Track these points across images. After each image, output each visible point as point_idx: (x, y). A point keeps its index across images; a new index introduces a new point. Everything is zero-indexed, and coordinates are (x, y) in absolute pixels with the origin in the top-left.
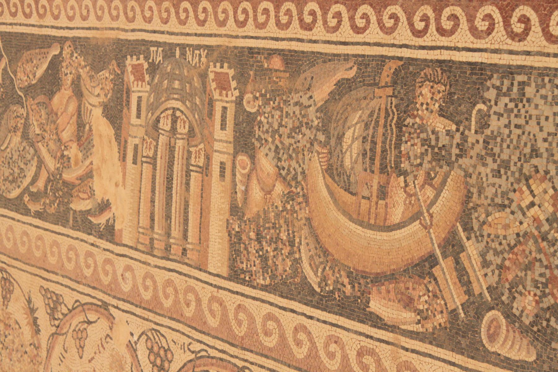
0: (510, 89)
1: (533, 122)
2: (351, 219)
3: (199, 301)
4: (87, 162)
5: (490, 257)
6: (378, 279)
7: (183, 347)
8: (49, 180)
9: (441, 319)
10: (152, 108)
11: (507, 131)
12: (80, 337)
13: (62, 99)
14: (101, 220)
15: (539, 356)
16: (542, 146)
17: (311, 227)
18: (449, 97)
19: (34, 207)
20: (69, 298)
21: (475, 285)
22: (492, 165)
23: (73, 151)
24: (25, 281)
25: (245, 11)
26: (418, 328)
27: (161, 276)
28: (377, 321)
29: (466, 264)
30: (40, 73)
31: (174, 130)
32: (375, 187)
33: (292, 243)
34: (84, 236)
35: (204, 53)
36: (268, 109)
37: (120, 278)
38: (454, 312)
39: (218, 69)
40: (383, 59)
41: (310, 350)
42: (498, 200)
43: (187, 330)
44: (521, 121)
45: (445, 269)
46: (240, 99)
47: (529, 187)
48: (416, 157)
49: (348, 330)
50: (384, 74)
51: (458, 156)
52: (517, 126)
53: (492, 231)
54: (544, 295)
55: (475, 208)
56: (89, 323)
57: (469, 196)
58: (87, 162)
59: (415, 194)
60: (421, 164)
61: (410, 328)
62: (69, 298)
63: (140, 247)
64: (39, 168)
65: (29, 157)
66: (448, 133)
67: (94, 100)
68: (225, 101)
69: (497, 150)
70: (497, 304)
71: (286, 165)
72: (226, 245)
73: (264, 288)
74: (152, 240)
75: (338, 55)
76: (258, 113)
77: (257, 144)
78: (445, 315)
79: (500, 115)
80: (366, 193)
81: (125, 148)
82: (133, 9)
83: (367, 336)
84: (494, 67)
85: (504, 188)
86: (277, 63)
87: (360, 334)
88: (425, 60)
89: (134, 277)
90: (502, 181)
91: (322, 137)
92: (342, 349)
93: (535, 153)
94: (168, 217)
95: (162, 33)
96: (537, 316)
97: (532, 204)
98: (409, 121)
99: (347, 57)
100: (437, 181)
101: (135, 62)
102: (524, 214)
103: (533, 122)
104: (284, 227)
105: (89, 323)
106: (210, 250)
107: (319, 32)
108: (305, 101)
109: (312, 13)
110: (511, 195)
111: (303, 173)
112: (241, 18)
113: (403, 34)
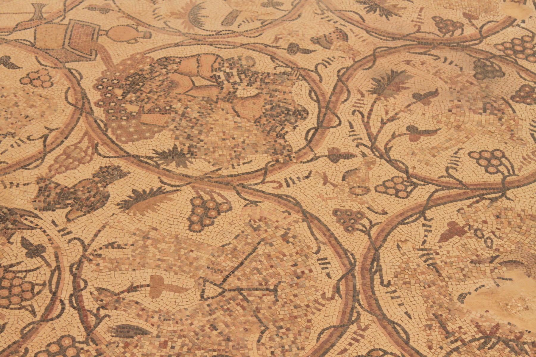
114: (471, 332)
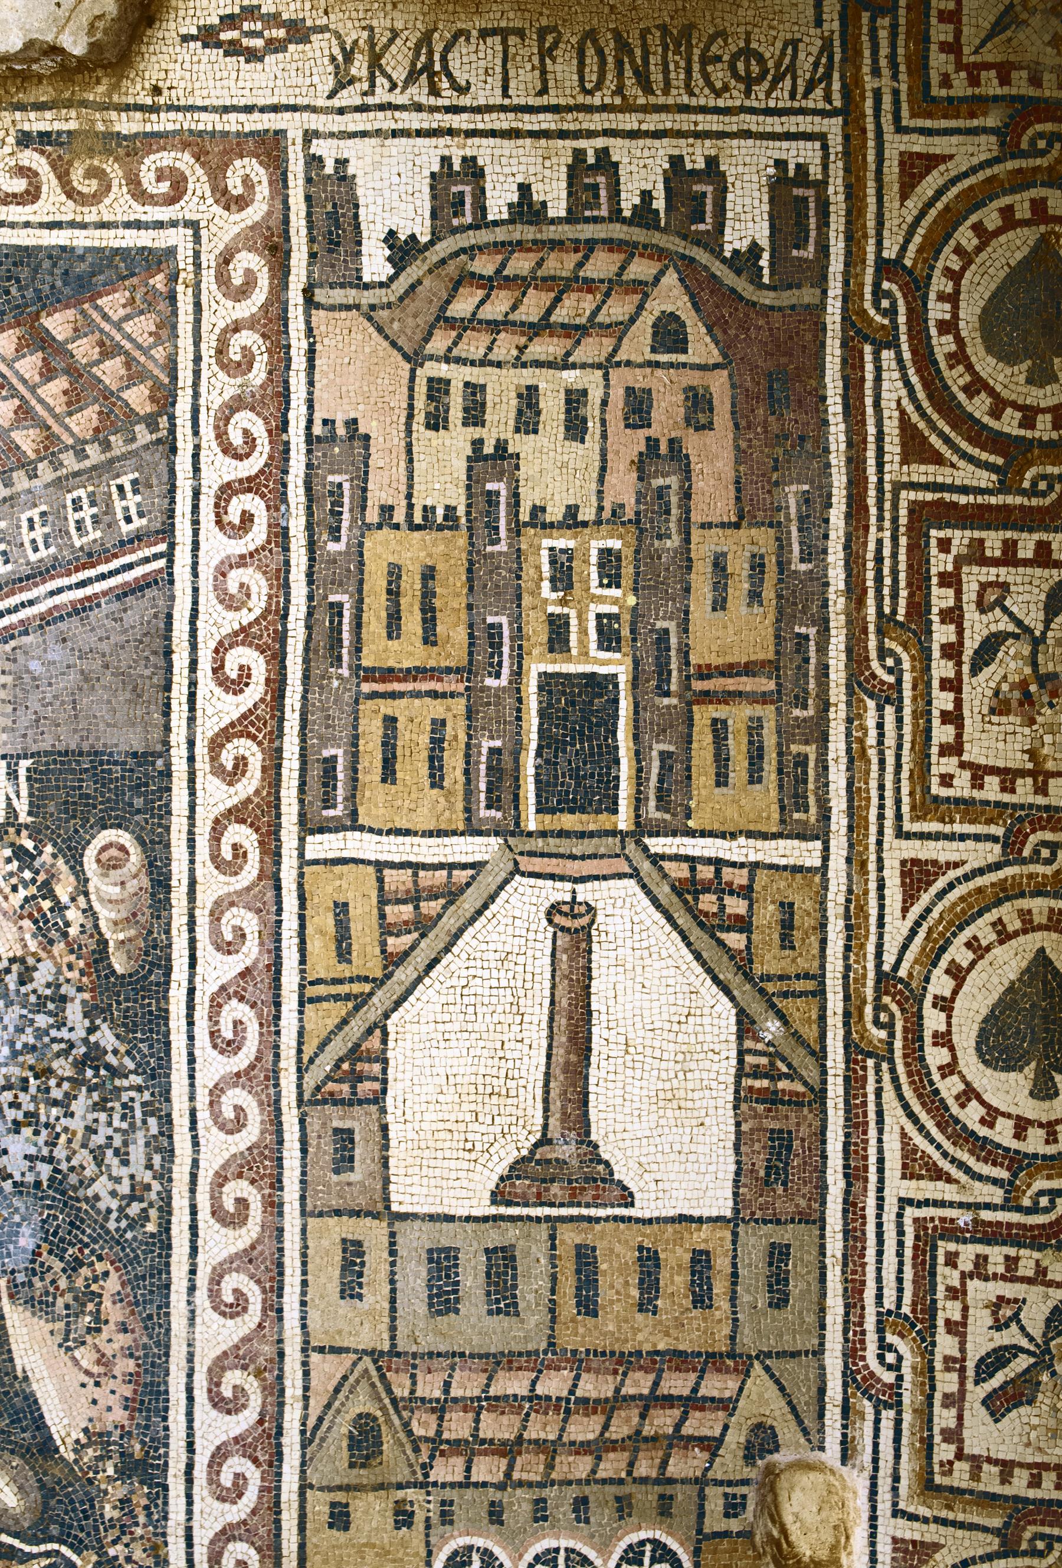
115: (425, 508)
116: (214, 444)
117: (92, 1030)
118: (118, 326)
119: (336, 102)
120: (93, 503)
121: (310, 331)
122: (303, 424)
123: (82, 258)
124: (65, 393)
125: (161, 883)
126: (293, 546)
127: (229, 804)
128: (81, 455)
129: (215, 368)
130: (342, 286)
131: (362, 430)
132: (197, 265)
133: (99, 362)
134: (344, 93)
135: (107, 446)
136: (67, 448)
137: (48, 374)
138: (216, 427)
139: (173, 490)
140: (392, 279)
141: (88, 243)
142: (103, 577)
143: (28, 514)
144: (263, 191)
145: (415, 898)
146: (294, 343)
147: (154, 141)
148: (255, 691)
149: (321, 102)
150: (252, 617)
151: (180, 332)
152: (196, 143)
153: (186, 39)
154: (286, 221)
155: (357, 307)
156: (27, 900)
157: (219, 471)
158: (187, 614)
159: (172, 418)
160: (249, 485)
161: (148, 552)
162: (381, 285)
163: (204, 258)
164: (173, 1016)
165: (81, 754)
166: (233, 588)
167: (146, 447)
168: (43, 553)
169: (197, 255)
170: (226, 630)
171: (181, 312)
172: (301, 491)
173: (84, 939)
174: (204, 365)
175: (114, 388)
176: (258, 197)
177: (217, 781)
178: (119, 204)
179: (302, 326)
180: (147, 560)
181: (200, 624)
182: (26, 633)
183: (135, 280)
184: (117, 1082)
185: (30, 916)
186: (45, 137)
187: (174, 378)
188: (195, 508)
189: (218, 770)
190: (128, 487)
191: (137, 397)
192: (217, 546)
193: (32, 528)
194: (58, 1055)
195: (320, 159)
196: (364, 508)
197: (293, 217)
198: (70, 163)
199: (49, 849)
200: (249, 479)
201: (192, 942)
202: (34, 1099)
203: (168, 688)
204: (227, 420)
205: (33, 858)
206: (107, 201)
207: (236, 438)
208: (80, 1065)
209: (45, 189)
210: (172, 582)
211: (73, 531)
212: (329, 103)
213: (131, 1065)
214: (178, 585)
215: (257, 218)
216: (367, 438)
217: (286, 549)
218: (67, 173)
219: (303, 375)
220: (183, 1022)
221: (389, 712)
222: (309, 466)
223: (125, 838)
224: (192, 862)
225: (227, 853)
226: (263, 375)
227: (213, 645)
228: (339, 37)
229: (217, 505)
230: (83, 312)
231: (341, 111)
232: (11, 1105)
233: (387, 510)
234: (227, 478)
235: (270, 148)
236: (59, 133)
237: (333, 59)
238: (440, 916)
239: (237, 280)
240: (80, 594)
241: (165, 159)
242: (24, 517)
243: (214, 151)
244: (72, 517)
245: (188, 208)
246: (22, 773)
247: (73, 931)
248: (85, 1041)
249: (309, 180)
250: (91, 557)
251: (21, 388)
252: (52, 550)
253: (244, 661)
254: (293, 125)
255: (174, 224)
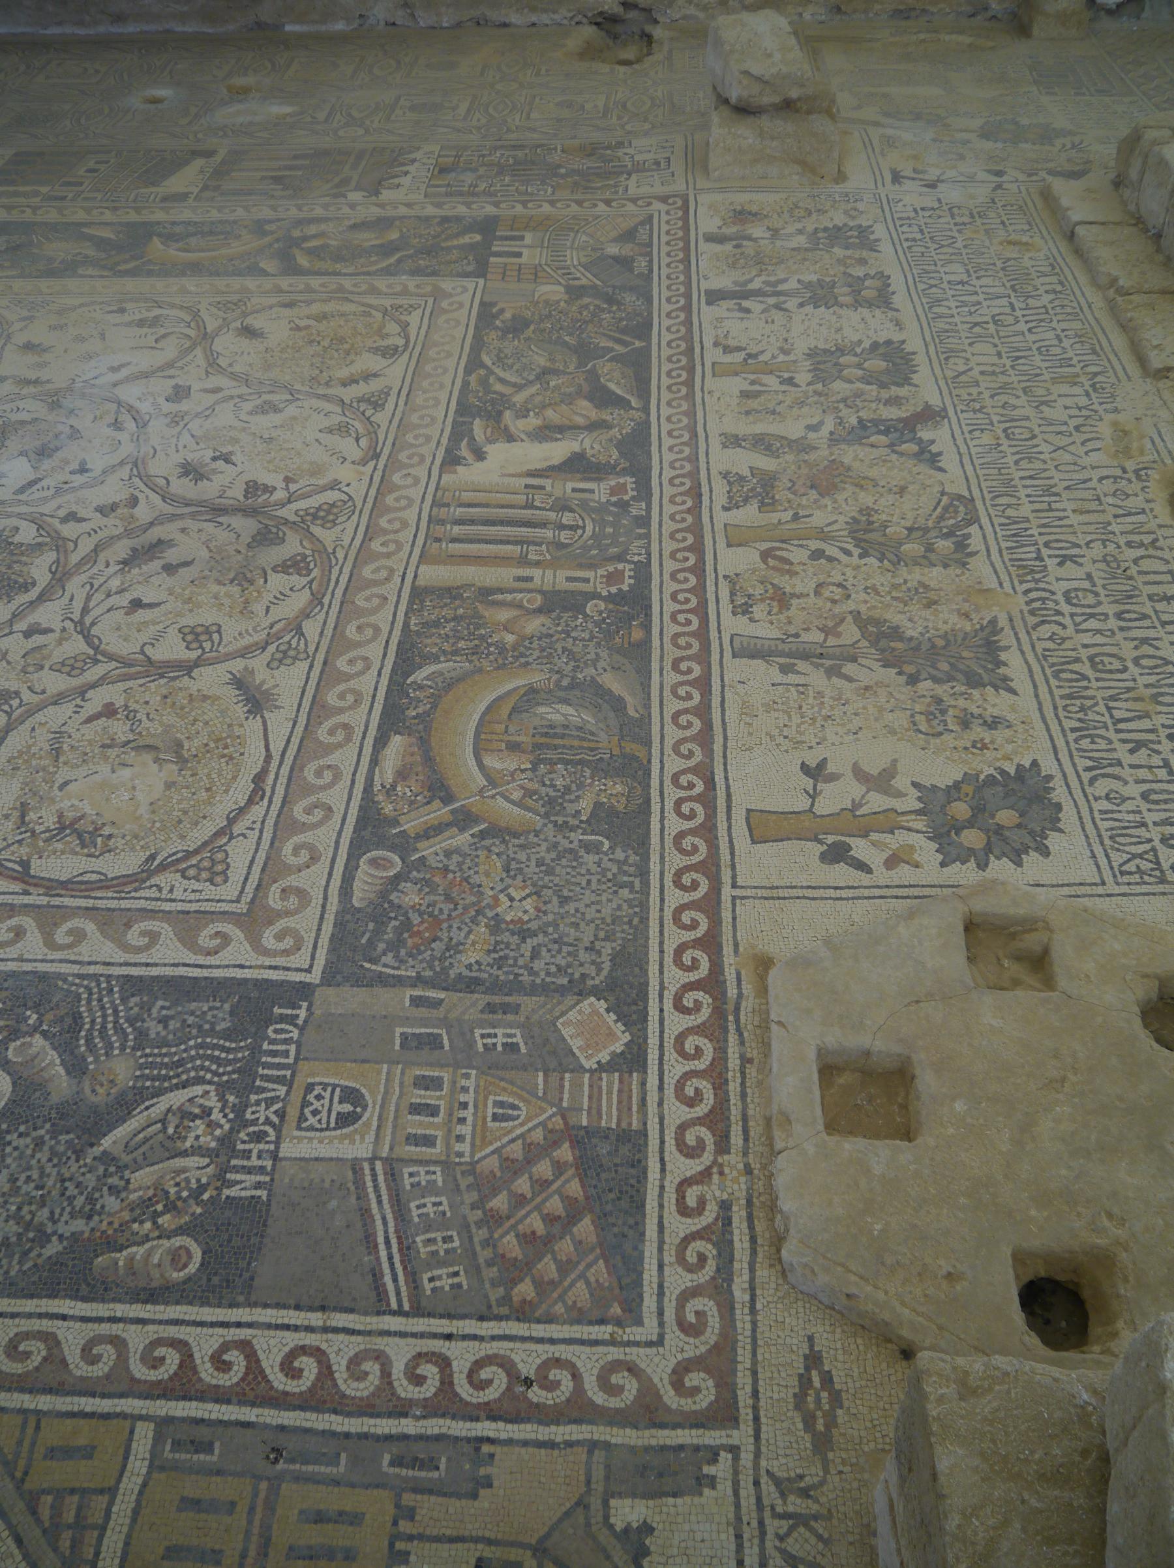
0: (625, 873)
1: (593, 898)
2: (484, 714)
3: (388, 555)
4: (523, 436)
5: (456, 858)
6: (424, 743)
7: (339, 539)
8: (502, 395)
9: (388, 809)
10: (584, 504)
11: (583, 872)
12: (342, 429)
13: (585, 410)
14: (464, 452)
15: (359, 910)
16: (571, 907)
17: (473, 672)
18: (612, 813)
19: (473, 379)
20: (381, 418)
21: (425, 844)
22: (548, 857)
23: (533, 421)
24: (395, 372)
25: (687, 601)
26: (377, 787)
27: (411, 515)
28: (381, 742)
29: (447, 834)
30: (612, 386)
31: (563, 527)
32: (518, 739)
33: (455, 653)
34: (447, 434)
35: (642, 558)
36: (590, 625)
37: (405, 472)
38: (395, 822)
39: (627, 574)
40: (648, 744)
41: (346, 674)
42: (513, 865)
43: (357, 543)
44: (594, 886)
45: (439, 812)
46: (598, 596)
47: (528, 895)
48: (552, 780)
49: (370, 713)
50: (634, 746)
51: (555, 823)
52: (589, 882)
53: (482, 858)
54: (421, 914)
55: (504, 841)
56: (357, 440)
57: (516, 835)
58: (523, 436)
59: (514, 780)
60: (544, 785)
61: (376, 778)
62: (381, 418)
63: (440, 493)
64: (514, 385)
65: (525, 374)
66: (578, 812)
67: (587, 444)
68: (595, 580)
69: (564, 862)
70: (408, 866)
71: (535, 645)
72: (449, 584)
73: (406, 624)
74: (448, 505)
75: (649, 698)
76: (586, 616)
77: (554, 615)
78: (393, 814)
79: (599, 864)
80: (511, 729)
81: (540, 476)
82: (683, 484)
83: (365, 733)
84: (646, 858)
85: (526, 870)
86: (637, 635)
87: (367, 727)
88: (649, 786)
89: (407, 487)
90: (533, 867)
91: (565, 682)
92: (350, 708)
93: (564, 901)
94: (472, 522)
95: (661, 515)
96: (399, 907)
97: (512, 899)
98: (588, 772)
99: (648, 707)
100: (529, 802)
101: (629, 486)
102: (502, 891)
103: (593, 898)
104: (471, 645)
105: (357, 440)
106: (441, 567)
107: (671, 678)
108: (602, 664)
109: (689, 671)
110: (520, 878)
111: (528, 663)
112: (681, 597)
113: (674, 764)
114: (51, 821)
115: (408, 1553)
116: (482, 1353)
117: (61, 1237)
118: (582, 1276)
119: (764, 1479)
120: (447, 1251)
121: (569, 1444)
122: (491, 1434)
123: (635, 1248)
124: (533, 1233)
125: (151, 1296)
126: (391, 1421)
127: (197, 1356)
128: (486, 1243)
129: (544, 1357)
130: (607, 1478)
131: (482, 1492)
132: (629, 1344)
133: (555, 1259)
134: (773, 1488)
135: (490, 1264)
136: (491, 1233)
137: (550, 1219)
138: (496, 1356)
139: (450, 1316)
140: (611, 1527)
141: (647, 1254)
142: (390, 1258)
143: (445, 1202)
144: (687, 1404)
145: (80, 1524)
146: (561, 1429)
147: (727, 1308)
148: (279, 1381)
149: (763, 1463)
150: (340, 1382)
151: (576, 1328)
152: (725, 1346)
153: (811, 1339)
154: (662, 1426)
155: (589, 1491)
156: (167, 1193)
157: (461, 1356)
158: (351, 1326)
159: (507, 1318)
160: (447, 1382)
161: (404, 1294)
162: (606, 1517)
163: (635, 1350)
164: (50, 1302)
165: (262, 1236)
166: (367, 1366)
167: (486, 1296)
168: (415, 1212)
169: (637, 1344)
170: (333, 1358)
171: (591, 1329)
172: (436, 1431)
173: (127, 1234)
174: (547, 1347)
175: (534, 1271)
176: (683, 1401)
177: (216, 1346)
178: (678, 1280)
179: (574, 1437)
180: (398, 1293)
181: (341, 1337)
182: (358, 1198)
183: (617, 1291)
184: (17, 1257)
185: (155, 1195)
186: (728, 1222)
187: (539, 1322)
188: (435, 1336)
189: (225, 1347)
190: (456, 1280)
191: (525, 1289)
192: (400, 1353)
193: (434, 1204)
194: (52, 1213)
195: (714, 1460)
196: (415, 1490)
197: (666, 1432)
198: (709, 1240)
199: (199, 1210)
200: (451, 1383)
201: (99, 1320)
202: (28, 1194)
203: (297, 1307)
204: (501, 1366)
205: (196, 1198)
206: (680, 1270)
207: (485, 1374)
208: (40, 1230)
209: (689, 1221)
210: (378, 1313)
211: (428, 1236)
212: (763, 1472)
213: (25, 1268)
214: (375, 1319)
215: (665, 1399)
216: (475, 1496)
217: (390, 1415)
218: (702, 1238)
219: (533, 1436)
220: (43, 1310)
221: (238, 1508)
222: (457, 1439)
223: (192, 1268)
224: (161, 1322)
225: (160, 1352)
226: (535, 1400)
227: (324, 1346)
228: (822, 1483)
229: (433, 1354)
230: (592, 1250)
231: (756, 1483)
232: (29, 1177)
233: (411, 1514)
234: (454, 1364)
235: (724, 1413)
236: (731, 1233)
237: (801, 1477)
238: (55, 1550)
239: (615, 1379)
240: (381, 1240)
241: (714, 1321)
242: (443, 1199)
243: (719, 1361)
244: (438, 1235)
245: (673, 1335)
246: (258, 1193)
247: (136, 1226)
248: (55, 1233)
249: (697, 1448)
250: (407, 1250)
251: (539, 1199)
252: (416, 1219)
253: (305, 1373)
254: (742, 1436)
255: (661, 1324)
